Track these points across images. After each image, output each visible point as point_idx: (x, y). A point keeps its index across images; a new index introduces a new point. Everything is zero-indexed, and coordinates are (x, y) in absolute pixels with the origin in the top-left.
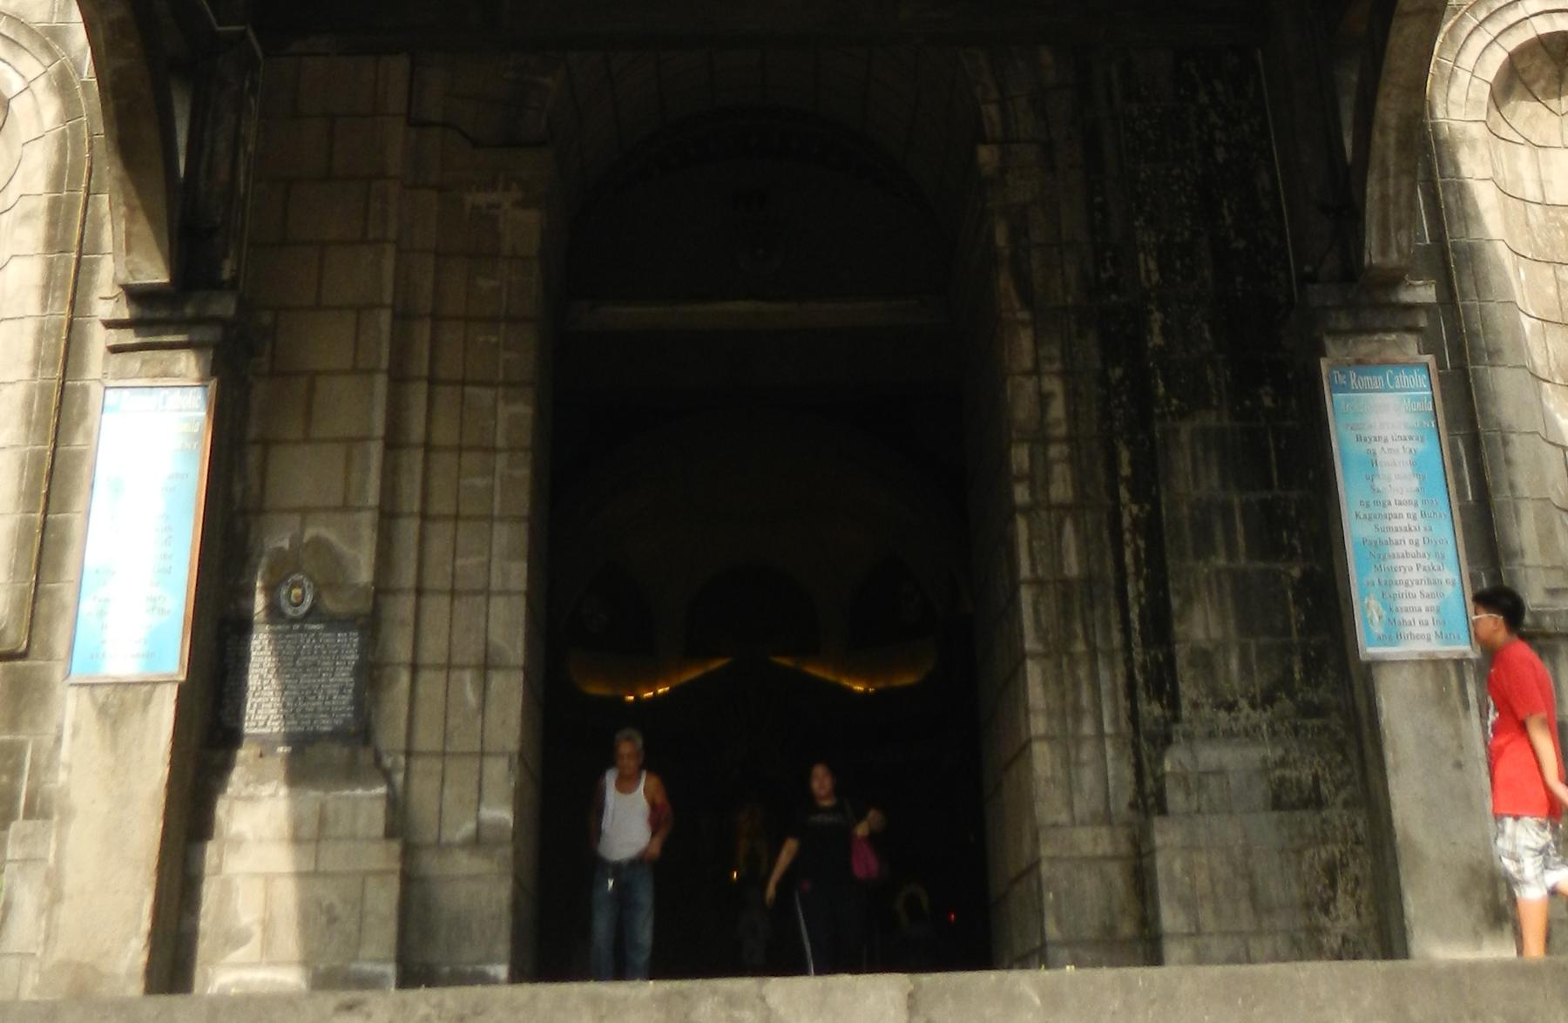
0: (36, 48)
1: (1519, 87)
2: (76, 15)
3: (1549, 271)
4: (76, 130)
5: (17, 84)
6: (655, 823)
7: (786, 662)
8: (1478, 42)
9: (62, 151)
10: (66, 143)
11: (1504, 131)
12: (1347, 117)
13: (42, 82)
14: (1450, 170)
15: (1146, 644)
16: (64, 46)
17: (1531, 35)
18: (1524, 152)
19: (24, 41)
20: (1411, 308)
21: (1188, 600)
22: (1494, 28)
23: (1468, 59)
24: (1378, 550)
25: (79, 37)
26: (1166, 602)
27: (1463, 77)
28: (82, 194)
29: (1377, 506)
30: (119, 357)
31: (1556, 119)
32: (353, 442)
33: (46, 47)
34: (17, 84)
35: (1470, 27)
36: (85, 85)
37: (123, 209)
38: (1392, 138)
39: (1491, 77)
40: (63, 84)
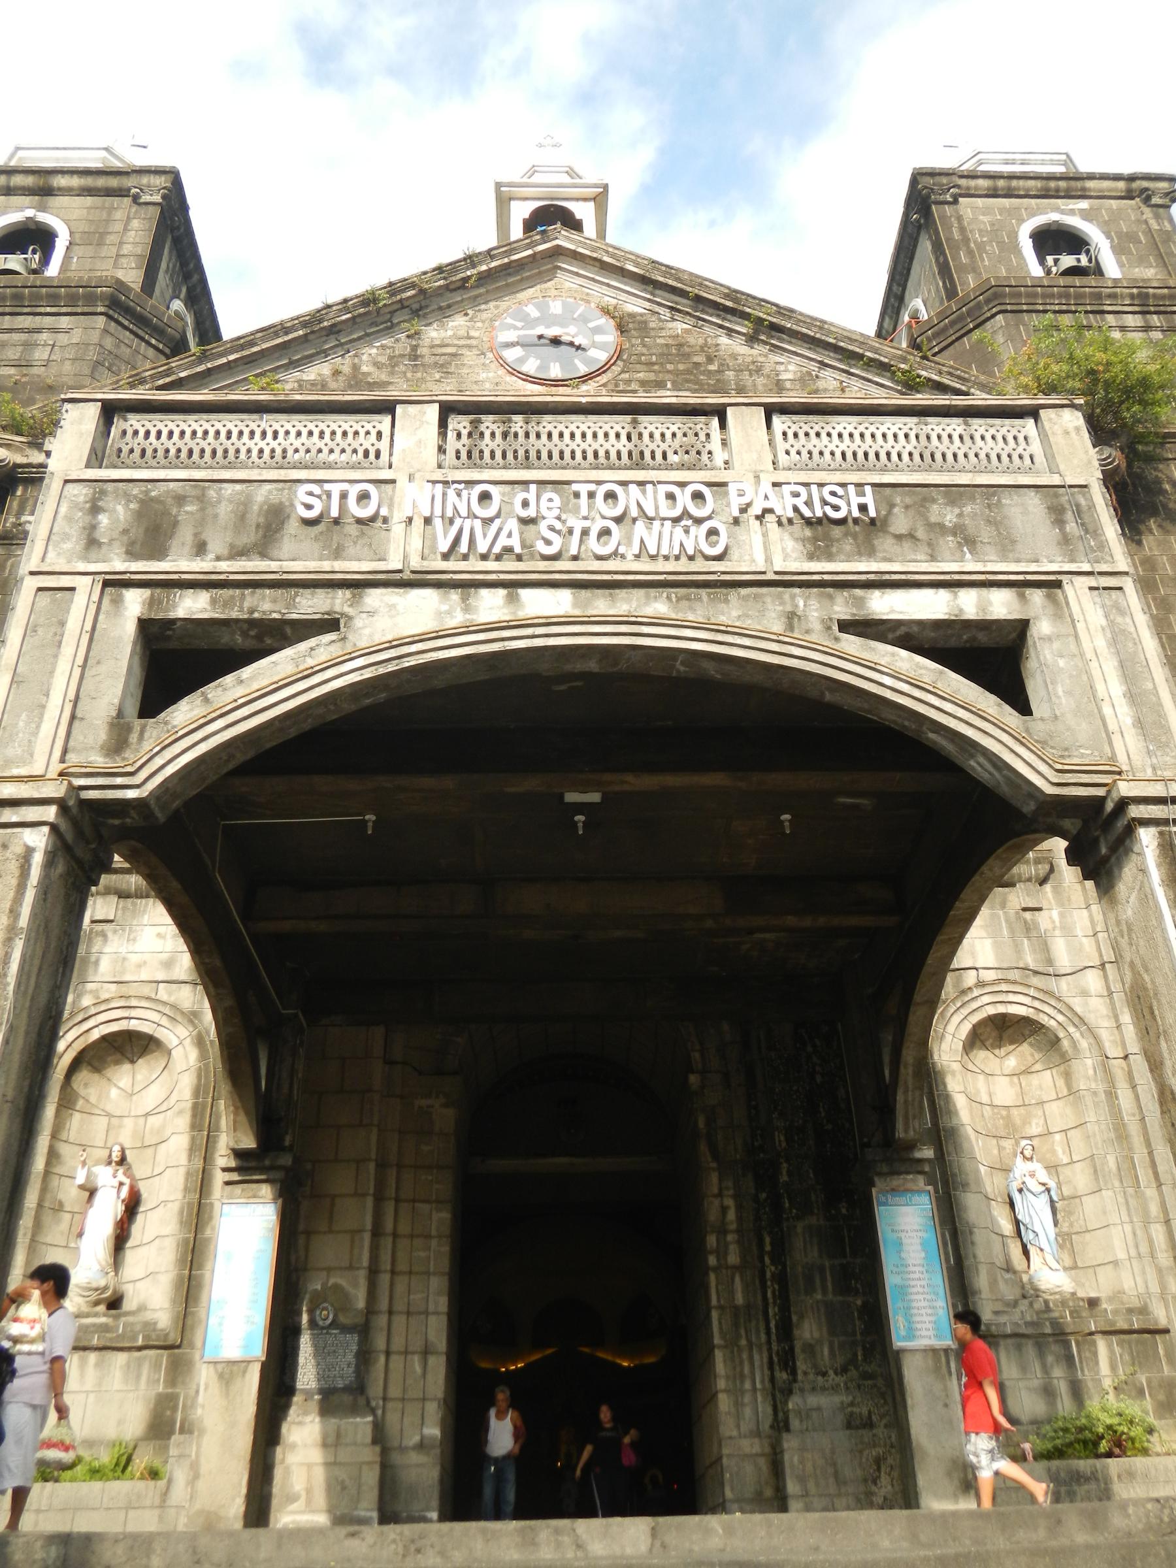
0: (185, 1022)
1: (978, 1043)
2: (207, 1004)
3: (994, 1141)
4: (207, 1065)
5: (175, 1041)
6: (516, 1436)
7: (586, 1350)
8: (956, 1019)
9: (199, 1077)
10: (201, 1073)
11: (970, 1066)
12: (886, 1059)
13: (188, 1040)
14: (941, 1087)
15: (779, 1341)
16: (201, 1021)
17: (985, 1015)
18: (981, 1077)
19: (179, 1018)
20: (920, 1161)
21: (801, 1317)
22: (965, 1011)
23: (951, 1028)
24: (903, 1290)
25: (208, 1016)
26: (790, 1318)
27: (949, 1038)
28: (210, 1100)
29: (903, 1265)
30: (230, 1187)
31: (998, 1060)
32: (356, 1232)
33: (191, 1022)
34: (175, 1041)
35: (952, 1011)
36: (211, 1042)
37: (232, 1108)
38: (910, 1070)
39: (963, 1038)
40: (200, 1041)
